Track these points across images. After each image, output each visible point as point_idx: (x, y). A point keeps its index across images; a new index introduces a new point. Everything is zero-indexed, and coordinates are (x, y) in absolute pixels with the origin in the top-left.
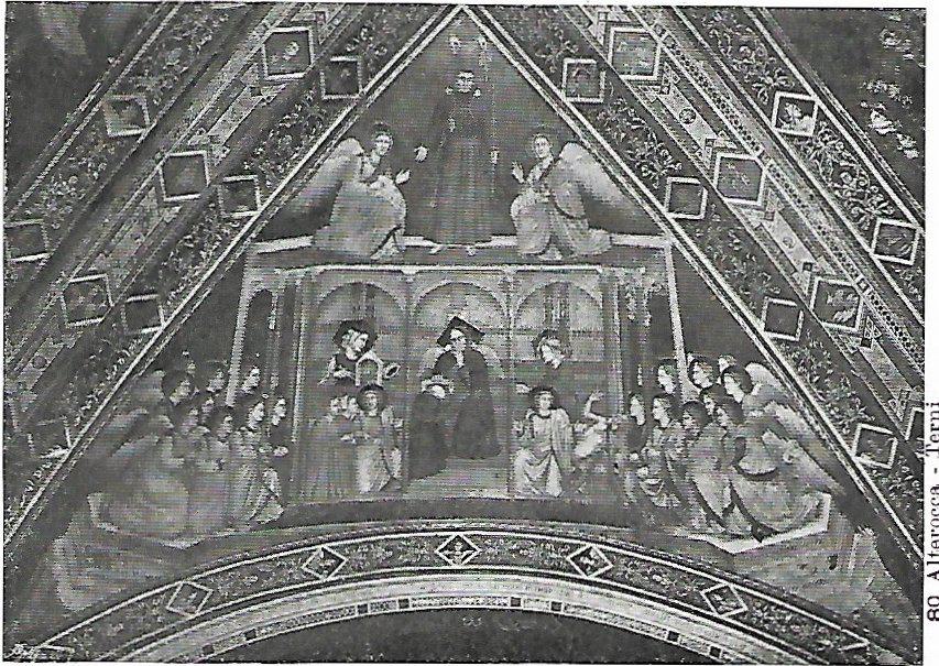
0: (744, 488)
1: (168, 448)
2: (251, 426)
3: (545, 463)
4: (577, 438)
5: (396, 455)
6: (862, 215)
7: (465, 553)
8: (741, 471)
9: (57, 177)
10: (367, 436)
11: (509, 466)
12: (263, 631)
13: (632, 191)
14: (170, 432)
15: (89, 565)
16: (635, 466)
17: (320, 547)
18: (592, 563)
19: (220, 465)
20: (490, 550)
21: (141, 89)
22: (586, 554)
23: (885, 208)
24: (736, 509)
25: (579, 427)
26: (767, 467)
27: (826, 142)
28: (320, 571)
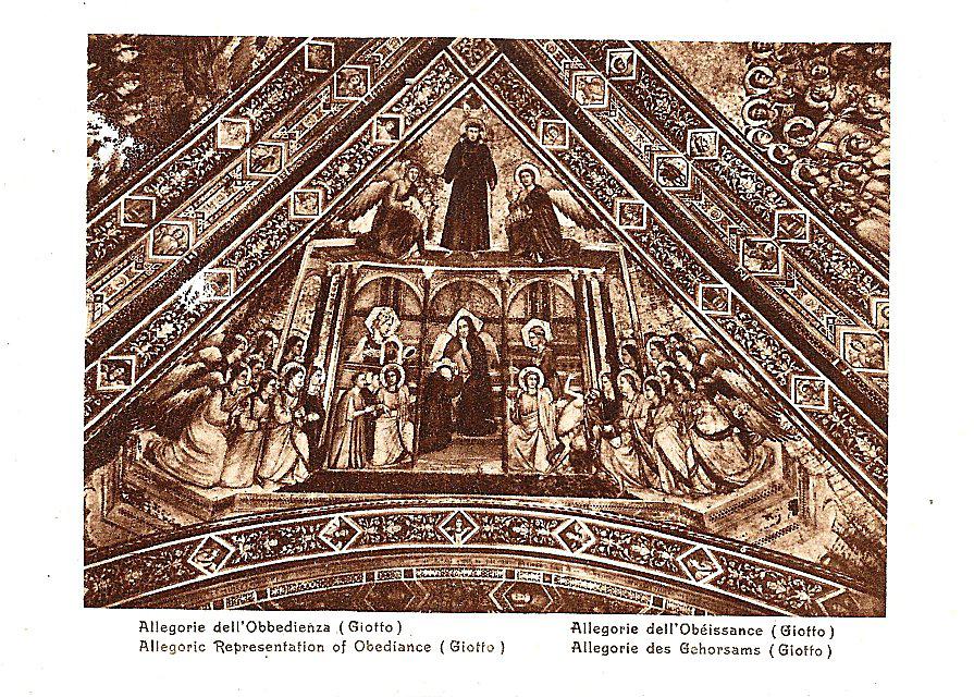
0: (705, 448)
1: (217, 400)
2: (292, 390)
3: (533, 439)
4: (560, 413)
5: (409, 428)
6: (763, 211)
7: (465, 530)
8: (701, 434)
9: (174, 168)
10: (386, 409)
11: (503, 441)
12: (275, 592)
13: (593, 211)
14: (221, 388)
15: (125, 501)
16: (609, 437)
17: (337, 515)
18: (577, 538)
19: (260, 424)
20: (487, 528)
21: (247, 116)
22: (570, 529)
23: (780, 202)
24: (701, 471)
25: (561, 403)
26: (721, 425)
27: (728, 161)
28: (335, 540)
